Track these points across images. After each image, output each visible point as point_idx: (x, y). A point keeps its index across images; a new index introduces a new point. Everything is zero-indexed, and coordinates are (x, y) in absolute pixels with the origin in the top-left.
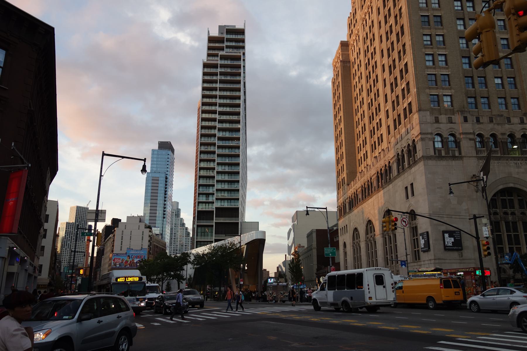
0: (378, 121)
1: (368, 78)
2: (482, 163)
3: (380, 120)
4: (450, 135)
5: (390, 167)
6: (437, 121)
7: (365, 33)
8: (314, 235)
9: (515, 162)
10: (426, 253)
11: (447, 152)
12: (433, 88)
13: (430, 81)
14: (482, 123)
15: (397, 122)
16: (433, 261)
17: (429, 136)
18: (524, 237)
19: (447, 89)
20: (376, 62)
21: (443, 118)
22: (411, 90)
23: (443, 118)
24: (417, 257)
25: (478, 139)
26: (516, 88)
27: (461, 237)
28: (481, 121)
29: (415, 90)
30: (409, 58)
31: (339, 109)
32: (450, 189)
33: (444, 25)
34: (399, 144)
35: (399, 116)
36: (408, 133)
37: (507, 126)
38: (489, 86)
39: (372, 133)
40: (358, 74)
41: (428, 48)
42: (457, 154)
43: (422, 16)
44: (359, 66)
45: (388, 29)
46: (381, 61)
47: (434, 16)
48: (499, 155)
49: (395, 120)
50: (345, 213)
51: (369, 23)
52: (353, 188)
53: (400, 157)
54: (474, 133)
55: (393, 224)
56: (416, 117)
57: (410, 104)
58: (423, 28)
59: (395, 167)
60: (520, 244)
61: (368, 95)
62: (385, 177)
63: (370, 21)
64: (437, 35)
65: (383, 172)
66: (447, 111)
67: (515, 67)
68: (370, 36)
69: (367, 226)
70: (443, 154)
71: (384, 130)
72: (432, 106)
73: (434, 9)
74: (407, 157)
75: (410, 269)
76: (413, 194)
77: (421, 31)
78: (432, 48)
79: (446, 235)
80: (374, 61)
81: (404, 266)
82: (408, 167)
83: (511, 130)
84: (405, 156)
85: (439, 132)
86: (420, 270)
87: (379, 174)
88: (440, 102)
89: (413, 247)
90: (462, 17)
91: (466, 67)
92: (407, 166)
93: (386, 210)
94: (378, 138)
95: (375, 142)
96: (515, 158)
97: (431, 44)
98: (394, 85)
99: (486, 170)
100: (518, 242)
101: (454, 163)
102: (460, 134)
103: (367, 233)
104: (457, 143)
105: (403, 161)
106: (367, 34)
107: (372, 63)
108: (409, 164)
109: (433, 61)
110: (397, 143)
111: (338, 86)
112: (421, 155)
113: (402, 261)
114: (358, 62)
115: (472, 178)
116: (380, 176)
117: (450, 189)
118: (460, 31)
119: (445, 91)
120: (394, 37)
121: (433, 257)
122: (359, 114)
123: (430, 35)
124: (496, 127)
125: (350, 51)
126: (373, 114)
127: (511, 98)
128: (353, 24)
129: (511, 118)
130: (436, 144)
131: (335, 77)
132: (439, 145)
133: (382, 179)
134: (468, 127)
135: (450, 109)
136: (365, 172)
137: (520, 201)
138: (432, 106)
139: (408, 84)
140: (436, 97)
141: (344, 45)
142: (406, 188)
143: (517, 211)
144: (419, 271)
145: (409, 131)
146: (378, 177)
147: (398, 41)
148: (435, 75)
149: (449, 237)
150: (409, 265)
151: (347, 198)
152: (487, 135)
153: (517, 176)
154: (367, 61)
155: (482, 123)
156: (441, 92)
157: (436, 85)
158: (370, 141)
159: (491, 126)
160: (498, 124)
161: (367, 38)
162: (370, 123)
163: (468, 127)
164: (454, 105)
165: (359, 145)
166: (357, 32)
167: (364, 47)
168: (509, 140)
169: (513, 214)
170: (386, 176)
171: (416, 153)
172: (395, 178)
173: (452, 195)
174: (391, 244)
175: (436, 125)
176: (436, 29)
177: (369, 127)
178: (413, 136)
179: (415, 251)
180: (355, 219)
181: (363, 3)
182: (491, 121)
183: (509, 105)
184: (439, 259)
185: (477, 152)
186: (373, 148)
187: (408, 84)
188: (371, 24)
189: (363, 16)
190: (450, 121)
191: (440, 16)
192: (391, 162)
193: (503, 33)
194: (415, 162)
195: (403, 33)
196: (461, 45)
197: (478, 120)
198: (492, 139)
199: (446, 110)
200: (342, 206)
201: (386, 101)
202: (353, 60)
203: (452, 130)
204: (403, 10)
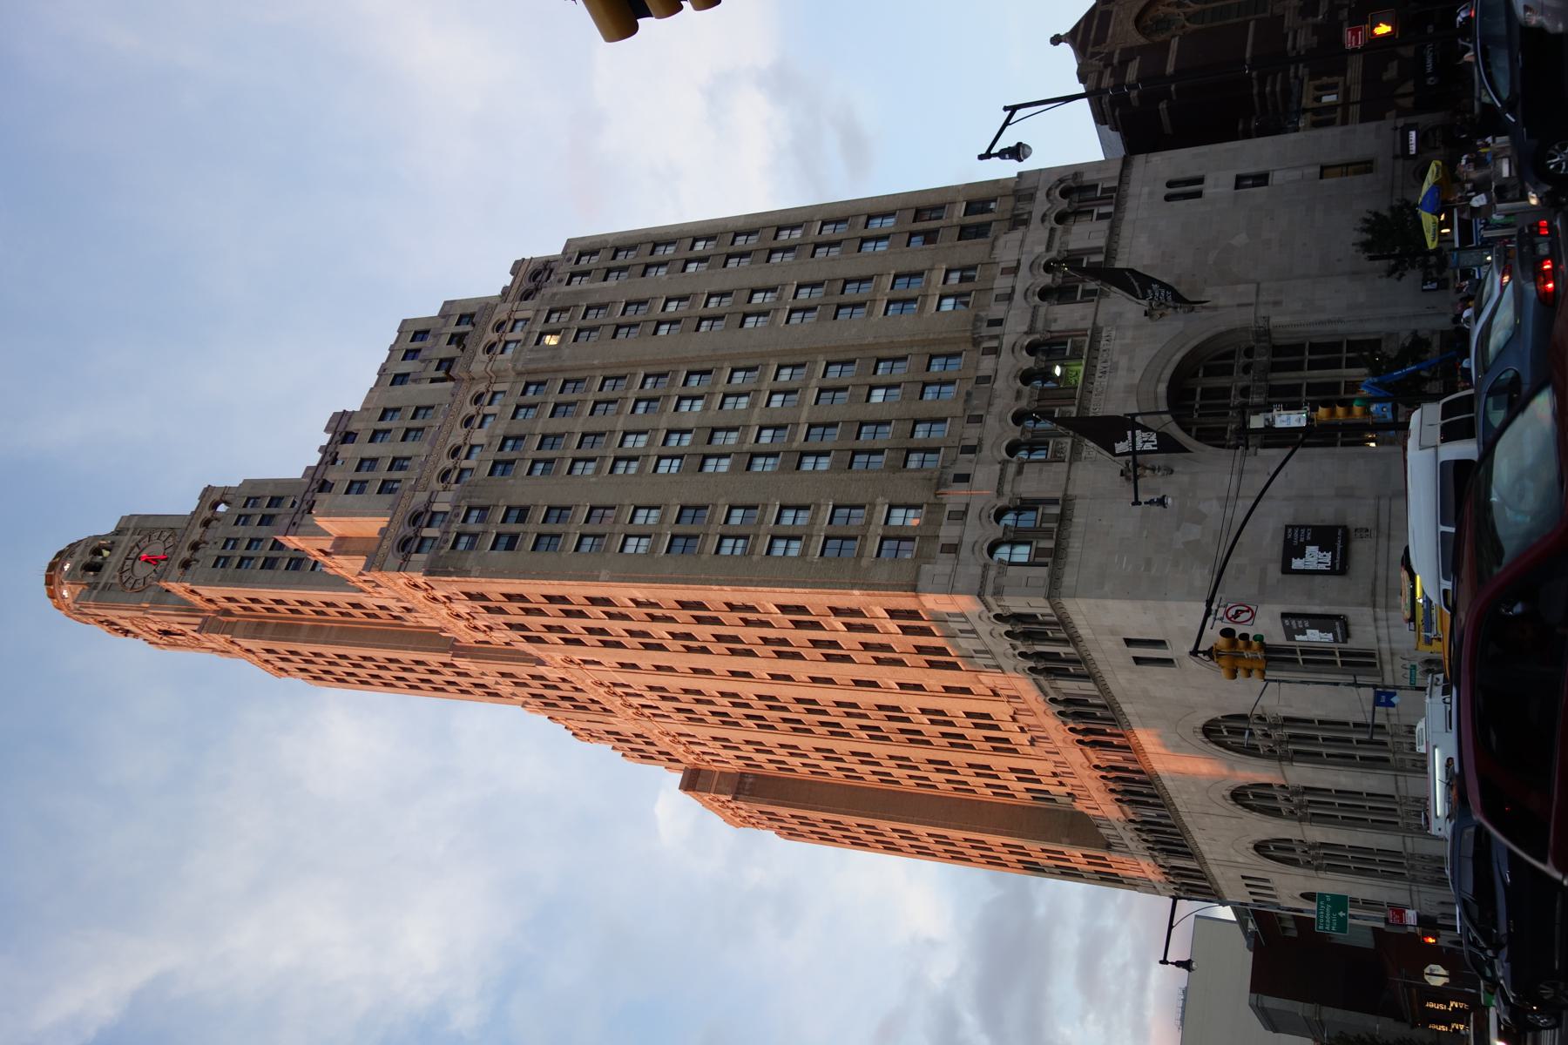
0: (925, 719)
1: (798, 727)
2: (1090, 448)
3: (923, 711)
4: (998, 521)
5: (1069, 701)
6: (952, 548)
7: (676, 716)
8: (1271, 1002)
9: (1098, 374)
10: (1353, 629)
11: (1047, 534)
12: (862, 547)
13: (840, 554)
14: (980, 440)
15: (937, 659)
16: (1381, 613)
17: (992, 573)
18: (1315, 372)
19: (871, 515)
20: (760, 697)
21: (948, 532)
22: (855, 606)
24: (1361, 663)
25: (1023, 454)
26: (904, 358)
27: (1306, 527)
28: (974, 442)
29: (856, 592)
30: (767, 599)
31: (871, 831)
32: (1151, 502)
33: (705, 501)
34: (1002, 661)
35: (920, 650)
36: (973, 631)
37: (999, 385)
38: (884, 416)
39: (958, 742)
40: (781, 754)
41: (753, 546)
42: (1056, 510)
43: (668, 551)
44: (760, 747)
45: (678, 645)
46: (762, 681)
47: (678, 521)
49: (932, 665)
50: (1201, 875)
51: (651, 698)
52: (1120, 830)
53: (1041, 665)
54: (1004, 463)
55: (1241, 643)
56: (932, 602)
57: (893, 614)
58: (701, 552)
59: (1069, 687)
60: (1338, 384)
61: (848, 735)
62: (1094, 721)
63: (648, 694)
64: (726, 522)
65: (1081, 727)
66: (931, 521)
67: (852, 356)
68: (687, 701)
69: (1252, 808)
70: (1050, 544)
71: (955, 706)
72: (910, 557)
73: (661, 520)
74: (1046, 647)
75: (1407, 683)
76: (1160, 643)
77: (704, 557)
78: (757, 536)
79: (1297, 564)
80: (756, 703)
81: (1395, 700)
82: (1076, 645)
84: (1039, 648)
85: (986, 546)
86: (1407, 614)
87: (1087, 739)
88: (903, 533)
89: (1330, 667)
90: (698, 460)
91: (824, 463)
92: (1070, 650)
93: (1201, 737)
94: (977, 726)
95: (988, 739)
96: (1089, 375)
97: (746, 537)
98: (832, 652)
99: (1108, 431)
100: (1333, 387)
101: (1079, 519)
102: (999, 493)
103: (1275, 812)
104: (1025, 505)
105: (1055, 657)
106: (679, 710)
107: (759, 708)
108: (1065, 642)
109: (790, 538)
110: (998, 667)
111: (804, 821)
112: (1044, 602)
113: (1377, 703)
114: (748, 750)
115: (1128, 479)
116: (1093, 737)
117: (1151, 502)
118: (732, 468)
119: (875, 520)
120: (704, 632)
121: (1368, 611)
122: (897, 772)
123: (722, 538)
124: (995, 409)
125: (716, 767)
126: (902, 731)
127: (928, 369)
128: (644, 747)
130: (1015, 559)
131: (776, 824)
132: (1022, 553)
133: (1103, 733)
134: (985, 475)
136: (1075, 782)
137: (1209, 372)
138: (908, 556)
139: (836, 611)
140: (886, 544)
141: (694, 781)
142: (1138, 660)
143: (1238, 381)
144: (1412, 619)
145: (967, 627)
146: (1093, 744)
147: (716, 621)
148: (827, 538)
149: (1302, 556)
150: (1389, 681)
151: (1153, 857)
152: (1014, 433)
153: (1138, 375)
154: (751, 723)
155: (980, 440)
156: (877, 529)
157: (855, 538)
158: (982, 752)
159: (990, 421)
160: (989, 405)
161: (690, 711)
162: (928, 743)
163: (985, 475)
164: (917, 501)
165: (989, 791)
166: (667, 739)
167: (713, 726)
168: (1038, 383)
169: (1245, 392)
170: (1092, 716)
171: (1035, 616)
172: (1104, 690)
173: (1169, 501)
174: (1316, 738)
175: (964, 552)
176: (710, 522)
177: (941, 748)
178: (984, 617)
179: (1343, 663)
180: (1226, 841)
181: (596, 707)
183: (944, 377)
184: (1374, 593)
185: (1057, 458)
186: (1002, 746)
187: (836, 611)
188: (655, 695)
189: (630, 711)
190: (960, 516)
191: (683, 508)
192: (1053, 695)
193: (763, 374)
194: (1063, 622)
195: (700, 605)
196: (768, 469)
197: (972, 450)
198: (1029, 424)
199: (927, 522)
200: (1178, 881)
201: (873, 684)
202: (741, 762)
203: (984, 515)
204: (641, 597)
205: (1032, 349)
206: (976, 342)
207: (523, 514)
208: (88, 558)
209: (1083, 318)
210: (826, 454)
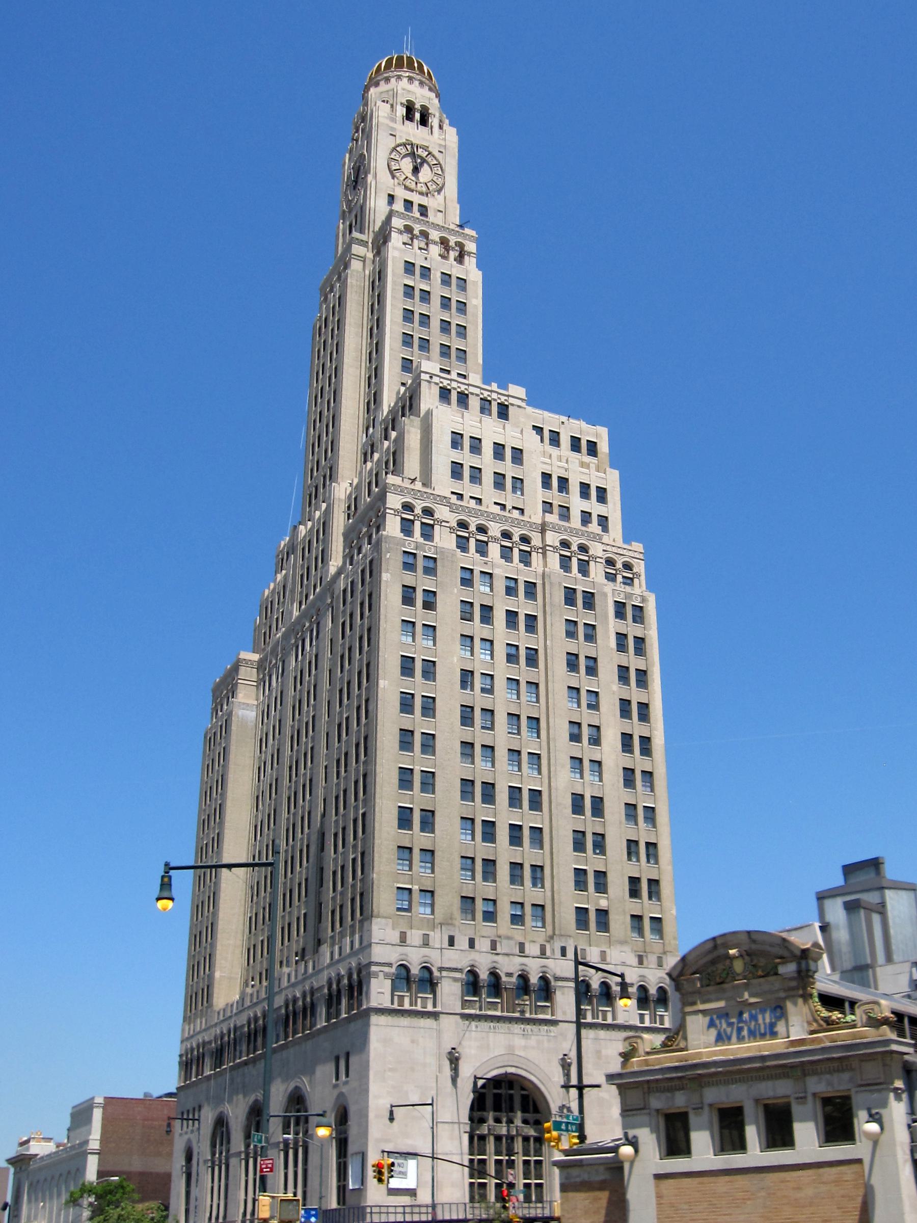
9: (522, 1026)
17: (386, 969)
21: (415, 937)
23: (415, 937)
48: (498, 1013)
83: (524, 967)
102: (441, 969)
129: (527, 946)
135: (428, 919)
153: (522, 1054)
185: (464, 1004)
190: (426, 944)
205: (544, 979)
207: (429, 605)
208: (418, 106)
209: (564, 1013)
210: (473, 839)
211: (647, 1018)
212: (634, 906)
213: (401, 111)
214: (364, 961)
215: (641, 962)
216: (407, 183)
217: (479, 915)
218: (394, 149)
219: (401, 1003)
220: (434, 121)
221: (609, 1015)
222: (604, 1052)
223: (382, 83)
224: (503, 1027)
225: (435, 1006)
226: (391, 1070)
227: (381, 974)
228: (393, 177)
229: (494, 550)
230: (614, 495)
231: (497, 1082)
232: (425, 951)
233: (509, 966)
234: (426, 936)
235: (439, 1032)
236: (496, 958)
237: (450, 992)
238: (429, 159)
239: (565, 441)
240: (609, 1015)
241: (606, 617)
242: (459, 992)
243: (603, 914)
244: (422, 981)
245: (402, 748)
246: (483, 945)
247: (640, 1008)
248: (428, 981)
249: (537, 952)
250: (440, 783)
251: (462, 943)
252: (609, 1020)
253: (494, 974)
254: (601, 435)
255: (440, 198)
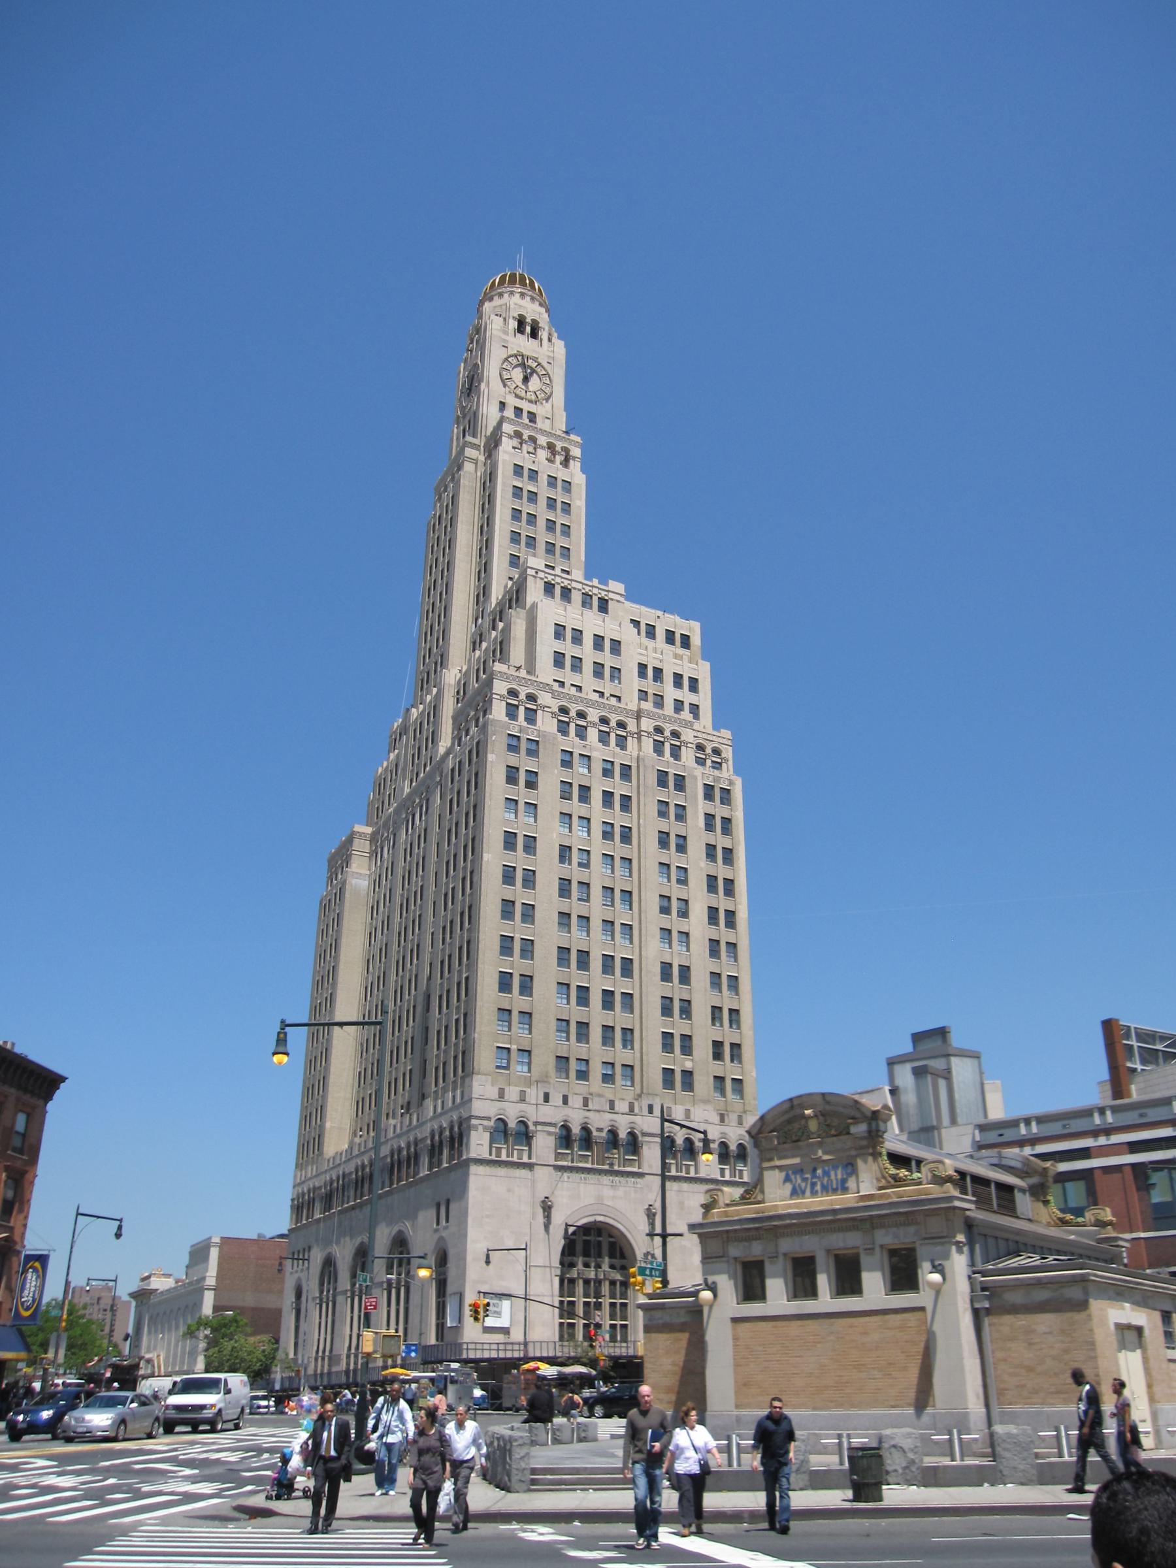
6: (501, 1094)
17: (485, 1123)
21: (512, 1093)
23: (512, 1093)
48: (589, 1166)
102: (536, 1123)
129: (617, 1103)
182: (586, 1102)
185: (558, 1156)
190: (523, 1099)
197: (565, 1100)
205: (632, 1134)
206: (639, 1096)
207: (531, 785)
208: (528, 320)
209: (650, 1166)
210: (568, 1003)
211: (727, 1173)
212: (717, 1068)
213: (513, 324)
214: (465, 1115)
215: (722, 1120)
216: (518, 391)
217: (573, 1074)
218: (506, 360)
219: (499, 1154)
220: (544, 334)
221: (692, 1169)
222: (686, 1203)
223: (496, 298)
224: (593, 1178)
225: (530, 1158)
226: (487, 1216)
227: (480, 1128)
228: (505, 385)
229: (593, 734)
230: (705, 685)
231: (586, 1229)
232: (522, 1106)
233: (600, 1122)
234: (523, 1093)
235: (533, 1182)
236: (588, 1114)
237: (544, 1145)
238: (539, 369)
239: (660, 634)
240: (692, 1169)
241: (696, 798)
242: (553, 1146)
243: (688, 1074)
244: (518, 1134)
245: (503, 917)
246: (576, 1101)
247: (721, 1162)
248: (524, 1135)
249: (627, 1110)
250: (538, 914)
251: (556, 1099)
252: (692, 1174)
253: (586, 1129)
254: (694, 630)
255: (548, 406)
